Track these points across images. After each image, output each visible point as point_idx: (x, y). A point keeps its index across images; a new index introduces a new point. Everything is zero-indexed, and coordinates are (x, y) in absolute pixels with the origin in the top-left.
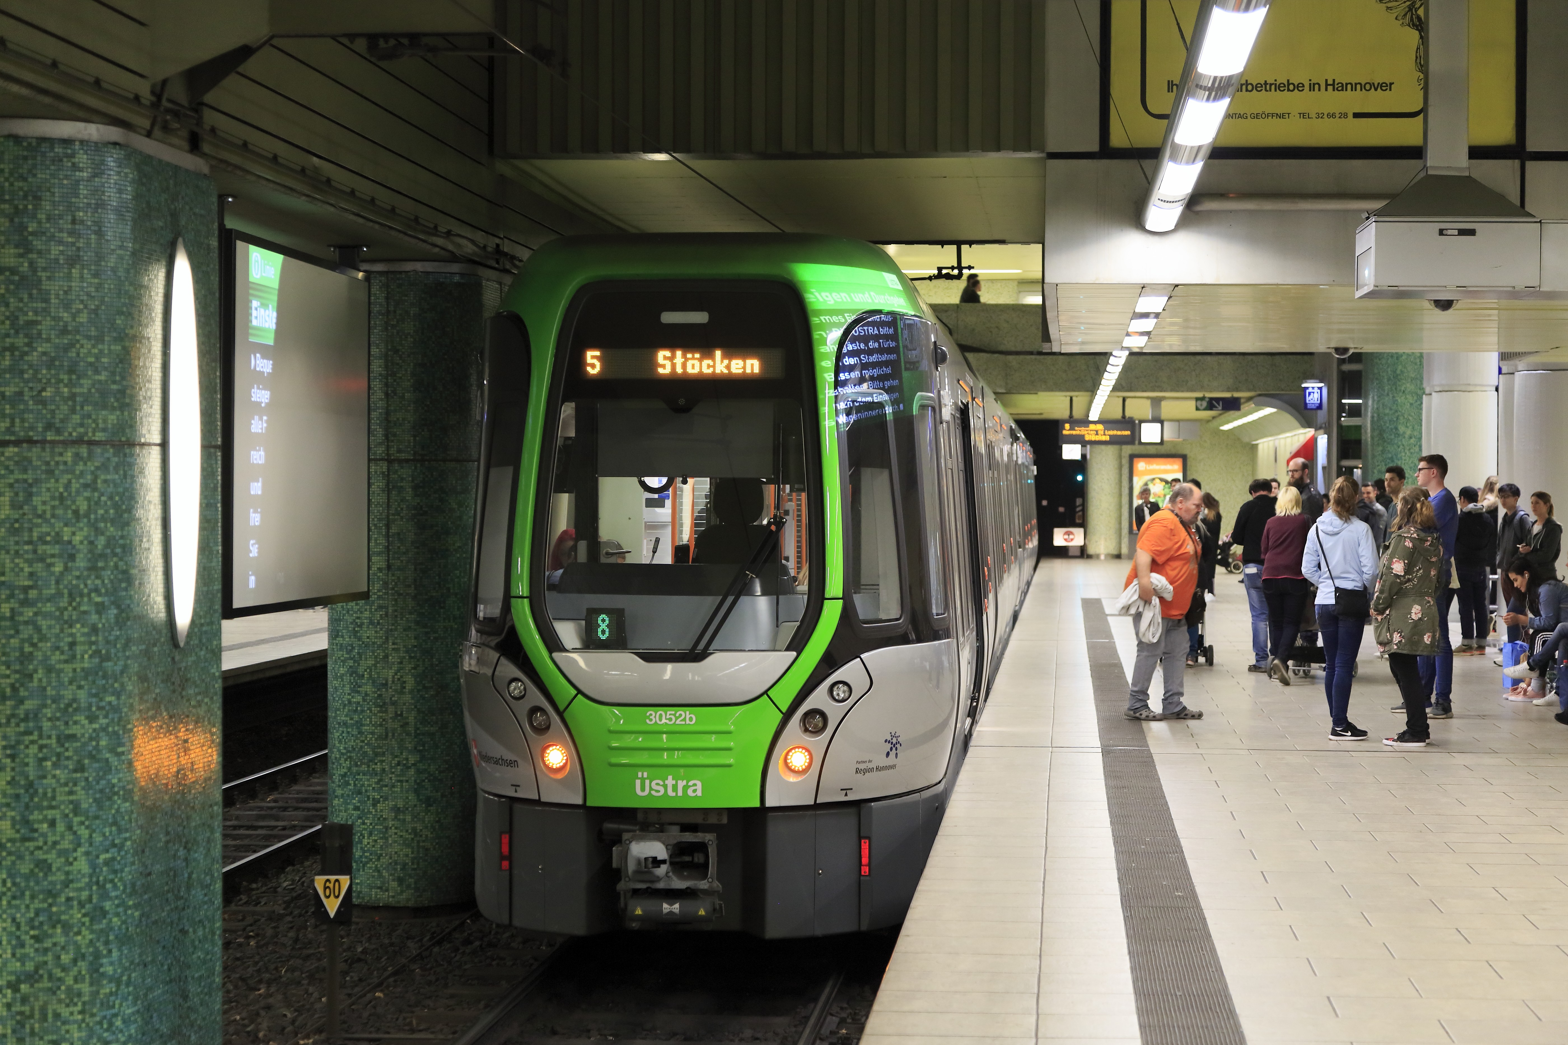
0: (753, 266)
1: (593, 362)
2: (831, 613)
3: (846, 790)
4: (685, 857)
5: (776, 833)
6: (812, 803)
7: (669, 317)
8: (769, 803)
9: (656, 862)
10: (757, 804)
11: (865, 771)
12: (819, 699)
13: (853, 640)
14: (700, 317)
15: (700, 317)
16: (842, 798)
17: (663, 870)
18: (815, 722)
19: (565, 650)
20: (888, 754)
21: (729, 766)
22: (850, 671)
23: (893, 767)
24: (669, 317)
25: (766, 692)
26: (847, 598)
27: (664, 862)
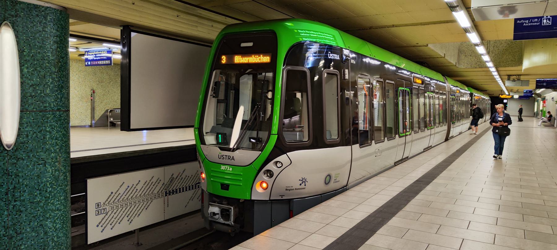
0: (267, 28)
1: (224, 59)
2: (274, 139)
3: (282, 196)
4: (225, 214)
5: (256, 207)
6: (268, 199)
7: (243, 45)
8: (253, 198)
9: (214, 214)
10: (250, 199)
11: (290, 190)
12: (271, 166)
13: (282, 148)
14: (251, 44)
15: (251, 44)
16: (280, 198)
17: (217, 217)
18: (270, 173)
19: (205, 144)
20: (301, 185)
21: (240, 185)
22: (283, 158)
23: (304, 188)
24: (243, 45)
25: (252, 163)
26: (279, 134)
27: (218, 214)
